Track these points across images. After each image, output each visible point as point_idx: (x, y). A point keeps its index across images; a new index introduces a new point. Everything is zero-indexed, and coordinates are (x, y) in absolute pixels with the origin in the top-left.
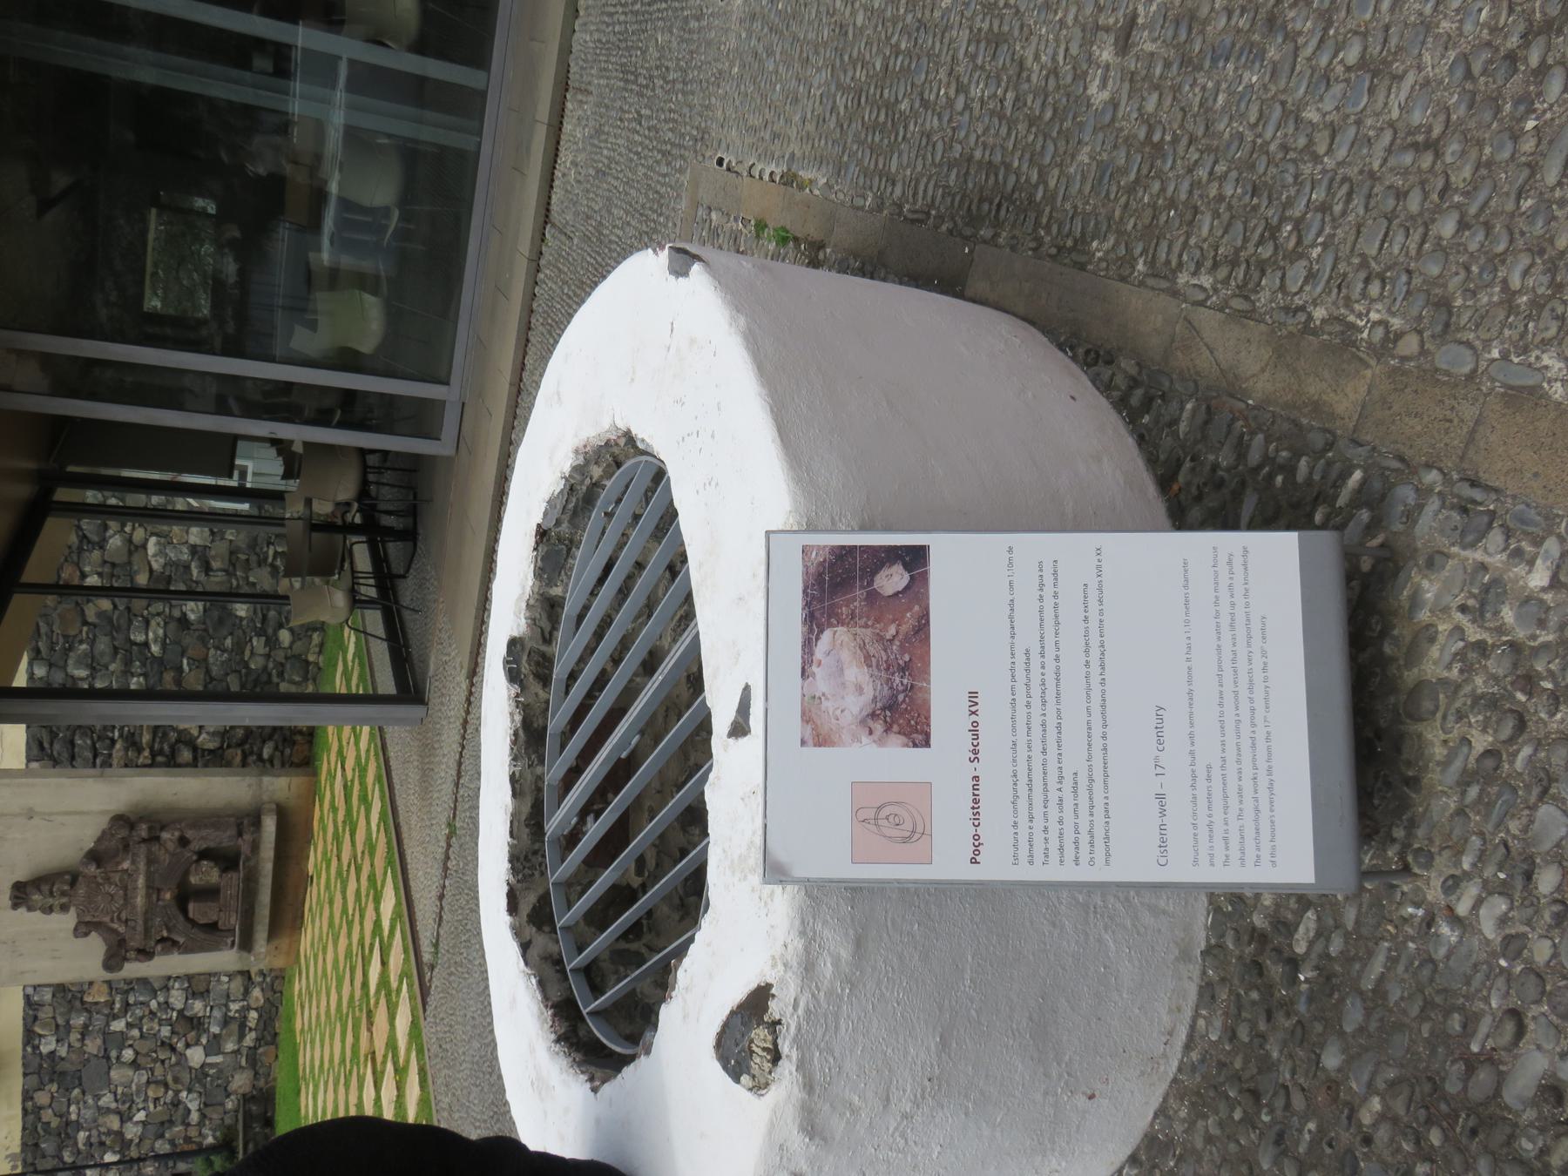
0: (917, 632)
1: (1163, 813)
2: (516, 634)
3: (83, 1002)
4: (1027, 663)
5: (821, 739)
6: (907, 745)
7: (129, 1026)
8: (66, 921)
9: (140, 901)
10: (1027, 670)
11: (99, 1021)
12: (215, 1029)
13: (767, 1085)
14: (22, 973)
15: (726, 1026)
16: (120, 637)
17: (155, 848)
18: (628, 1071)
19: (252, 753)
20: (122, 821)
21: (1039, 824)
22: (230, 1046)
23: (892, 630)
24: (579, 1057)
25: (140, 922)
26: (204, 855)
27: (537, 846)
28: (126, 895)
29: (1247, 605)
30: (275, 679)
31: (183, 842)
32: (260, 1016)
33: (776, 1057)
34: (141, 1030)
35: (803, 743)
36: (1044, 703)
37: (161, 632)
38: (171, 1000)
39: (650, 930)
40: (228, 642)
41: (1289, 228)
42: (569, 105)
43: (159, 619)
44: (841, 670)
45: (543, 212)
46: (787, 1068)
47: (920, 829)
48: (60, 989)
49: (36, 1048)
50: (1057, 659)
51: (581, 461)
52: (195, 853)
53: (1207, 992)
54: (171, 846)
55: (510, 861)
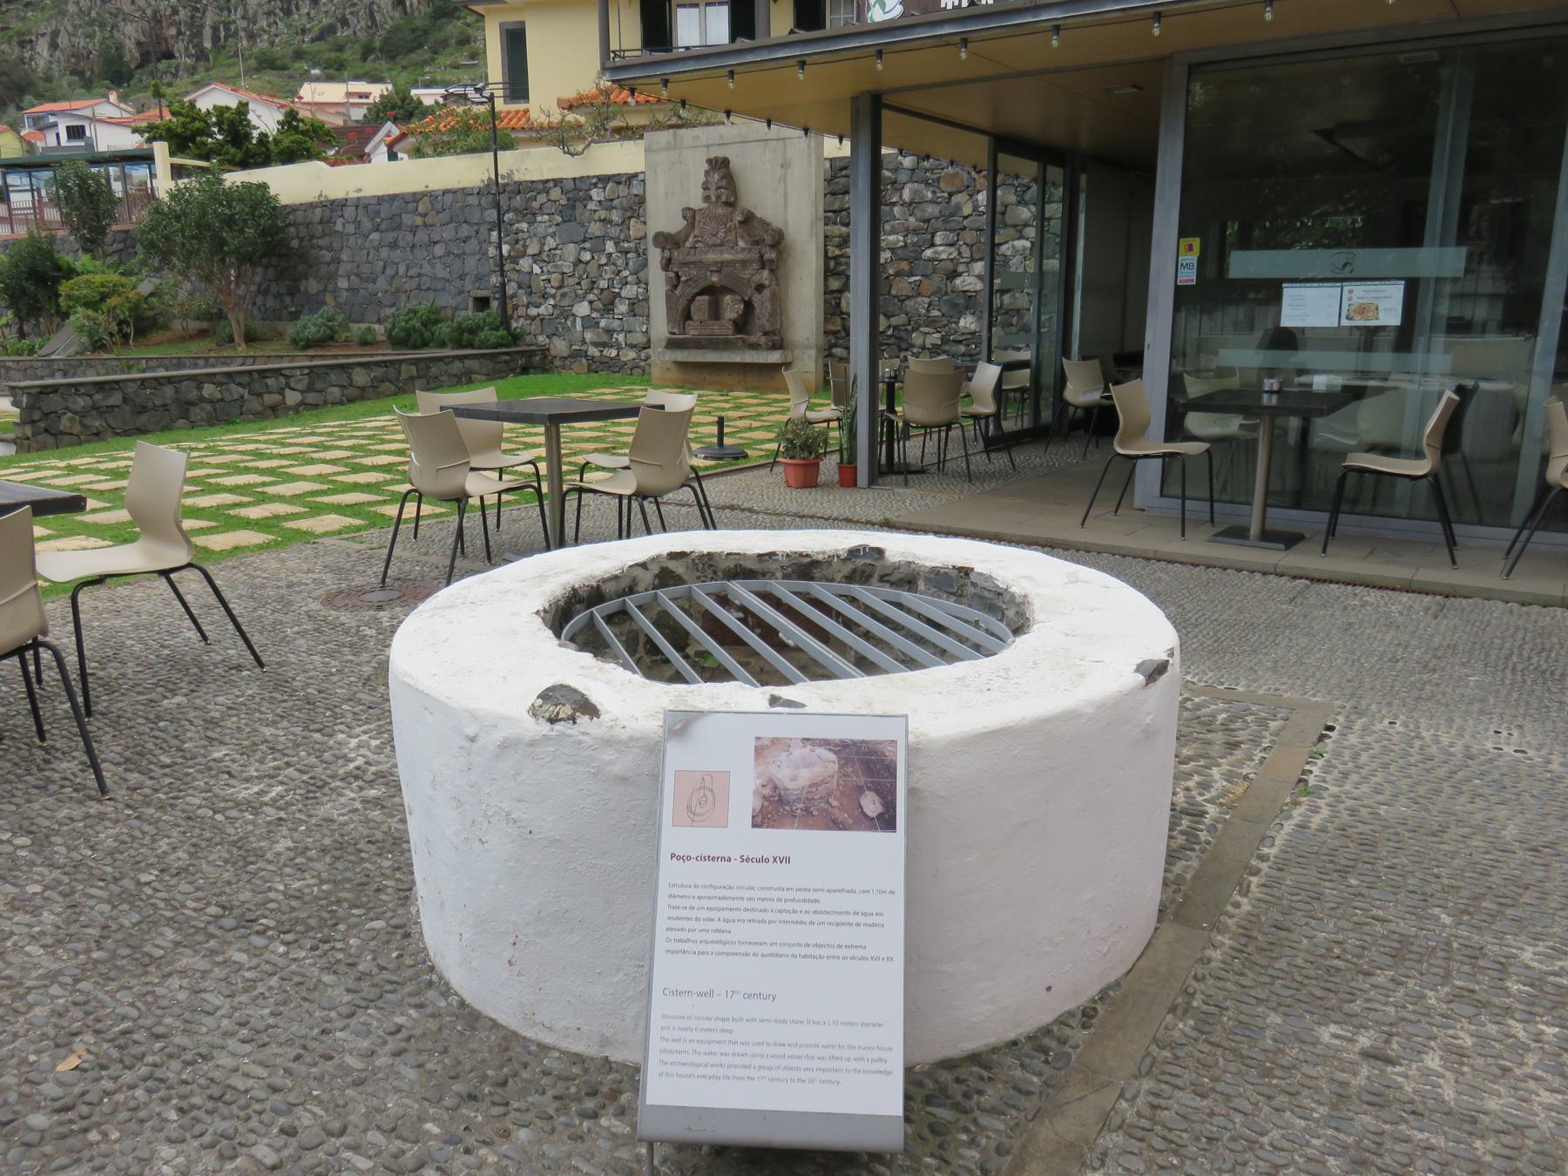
0: (833, 821)
1: (700, 994)
2: (887, 554)
3: (630, 218)
4: (810, 901)
5: (759, 751)
6: (754, 811)
7: (610, 255)
8: (696, 202)
9: (711, 257)
10: (804, 900)
11: (614, 231)
12: (603, 323)
13: (534, 715)
15: (575, 691)
16: (939, 223)
17: (755, 266)
18: (549, 633)
19: (837, 338)
20: (778, 240)
21: (697, 903)
22: (589, 336)
23: (835, 803)
24: (562, 603)
25: (694, 259)
26: (749, 305)
27: (720, 574)
29: (848, 1071)
31: (760, 288)
32: (612, 359)
33: (552, 721)
34: (606, 264)
35: (758, 738)
36: (780, 911)
37: (944, 256)
38: (629, 287)
39: (653, 661)
40: (935, 313)
41: (1175, 1162)
42: (1428, 599)
43: (955, 254)
44: (805, 766)
45: (1324, 577)
46: (545, 727)
47: (696, 818)
48: (641, 200)
49: (595, 185)
50: (812, 923)
51: (1018, 600)
53: (578, 1059)
54: (756, 278)
55: (709, 554)
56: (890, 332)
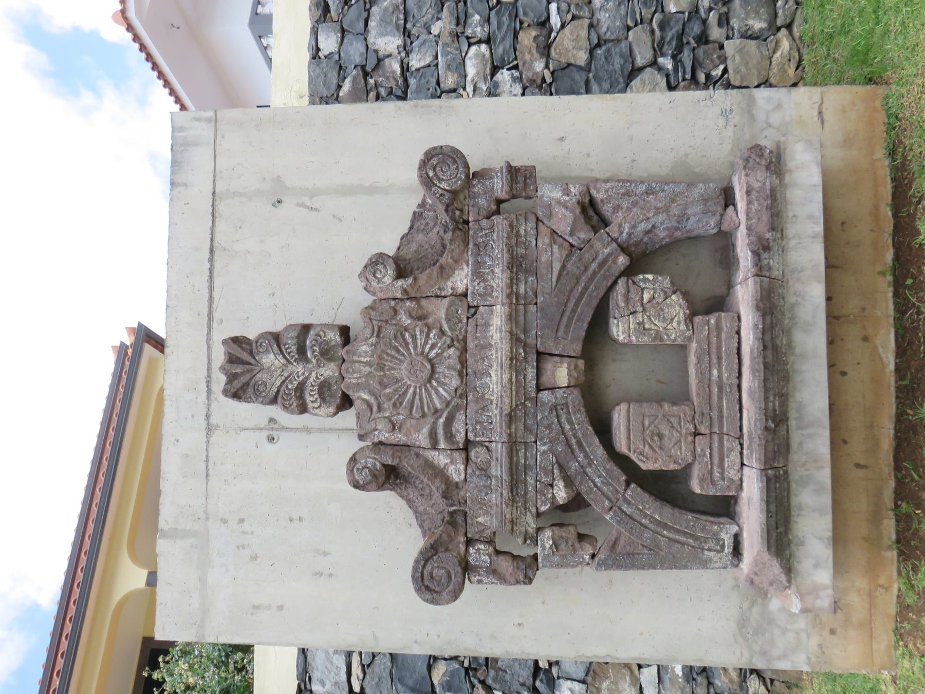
14: (256, 607)
25: (499, 449)
28: (463, 362)
30: (716, 33)
52: (624, 249)
56: (667, 62)
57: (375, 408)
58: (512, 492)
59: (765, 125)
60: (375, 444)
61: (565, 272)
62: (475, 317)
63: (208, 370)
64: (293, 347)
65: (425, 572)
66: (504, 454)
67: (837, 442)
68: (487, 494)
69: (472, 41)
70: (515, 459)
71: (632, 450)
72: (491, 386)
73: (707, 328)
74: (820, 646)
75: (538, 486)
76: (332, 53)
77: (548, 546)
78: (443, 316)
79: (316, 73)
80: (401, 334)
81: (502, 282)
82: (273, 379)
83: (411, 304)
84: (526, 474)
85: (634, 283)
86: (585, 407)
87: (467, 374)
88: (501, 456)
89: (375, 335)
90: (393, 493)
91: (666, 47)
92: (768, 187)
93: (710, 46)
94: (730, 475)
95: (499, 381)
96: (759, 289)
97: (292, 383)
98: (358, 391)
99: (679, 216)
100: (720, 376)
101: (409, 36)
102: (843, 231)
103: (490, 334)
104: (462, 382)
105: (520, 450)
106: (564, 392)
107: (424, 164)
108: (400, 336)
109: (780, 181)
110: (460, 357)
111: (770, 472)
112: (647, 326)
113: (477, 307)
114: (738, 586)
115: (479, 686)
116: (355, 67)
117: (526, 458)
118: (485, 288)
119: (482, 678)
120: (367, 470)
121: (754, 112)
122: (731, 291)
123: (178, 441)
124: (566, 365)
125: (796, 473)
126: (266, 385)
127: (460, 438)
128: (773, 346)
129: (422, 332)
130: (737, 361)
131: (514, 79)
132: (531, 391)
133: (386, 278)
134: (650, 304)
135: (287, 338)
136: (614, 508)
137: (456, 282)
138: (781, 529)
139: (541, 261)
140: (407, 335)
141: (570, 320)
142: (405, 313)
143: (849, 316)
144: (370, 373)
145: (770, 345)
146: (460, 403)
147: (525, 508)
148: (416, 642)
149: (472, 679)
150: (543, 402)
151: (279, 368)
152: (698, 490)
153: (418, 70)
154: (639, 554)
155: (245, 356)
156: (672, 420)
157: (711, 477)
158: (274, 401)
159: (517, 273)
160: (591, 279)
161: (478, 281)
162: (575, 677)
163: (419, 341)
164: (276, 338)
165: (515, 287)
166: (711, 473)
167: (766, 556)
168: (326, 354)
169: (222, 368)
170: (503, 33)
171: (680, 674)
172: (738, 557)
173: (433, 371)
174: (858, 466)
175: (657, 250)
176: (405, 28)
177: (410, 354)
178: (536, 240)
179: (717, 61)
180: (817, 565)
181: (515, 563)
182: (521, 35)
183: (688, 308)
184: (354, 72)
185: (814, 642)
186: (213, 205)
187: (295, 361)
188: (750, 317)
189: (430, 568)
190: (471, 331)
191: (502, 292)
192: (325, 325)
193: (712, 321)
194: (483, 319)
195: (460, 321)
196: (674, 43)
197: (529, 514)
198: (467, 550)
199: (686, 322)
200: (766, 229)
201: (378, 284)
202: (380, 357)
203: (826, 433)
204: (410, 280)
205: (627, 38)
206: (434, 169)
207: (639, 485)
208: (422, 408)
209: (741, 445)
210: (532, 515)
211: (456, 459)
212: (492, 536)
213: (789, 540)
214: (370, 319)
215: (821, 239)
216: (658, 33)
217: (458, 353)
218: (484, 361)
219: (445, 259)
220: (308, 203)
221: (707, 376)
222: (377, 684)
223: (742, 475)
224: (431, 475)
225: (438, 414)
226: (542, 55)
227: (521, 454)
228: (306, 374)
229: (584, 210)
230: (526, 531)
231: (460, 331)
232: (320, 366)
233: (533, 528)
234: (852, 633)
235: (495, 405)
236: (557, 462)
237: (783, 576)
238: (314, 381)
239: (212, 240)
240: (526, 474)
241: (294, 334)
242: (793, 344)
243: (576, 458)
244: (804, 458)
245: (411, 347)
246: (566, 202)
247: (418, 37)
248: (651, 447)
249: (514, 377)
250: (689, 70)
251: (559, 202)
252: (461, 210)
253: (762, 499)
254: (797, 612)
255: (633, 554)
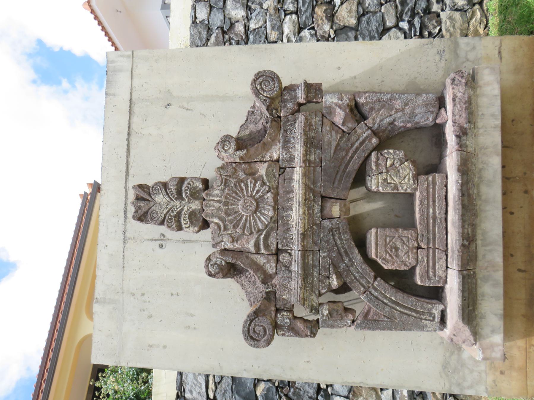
14: (151, 346)
25: (297, 254)
28: (276, 201)
52: (375, 133)
56: (404, 25)
57: (222, 228)
58: (304, 281)
59: (465, 60)
60: (222, 250)
61: (339, 148)
62: (283, 174)
63: (125, 204)
64: (174, 191)
65: (251, 328)
66: (300, 257)
67: (507, 256)
68: (289, 282)
69: (287, 12)
70: (306, 261)
71: (378, 257)
72: (293, 216)
73: (426, 183)
74: (494, 381)
75: (320, 278)
76: (204, 20)
77: (325, 314)
78: (265, 174)
79: (194, 32)
80: (239, 184)
81: (300, 153)
82: (162, 210)
83: (245, 166)
84: (313, 270)
85: (382, 155)
86: (350, 230)
87: (278, 209)
88: (298, 259)
89: (223, 184)
90: (233, 280)
91: (404, 16)
92: (466, 96)
93: (432, 15)
94: (439, 274)
95: (297, 213)
96: (459, 159)
97: (173, 213)
98: (212, 217)
99: (410, 114)
100: (434, 212)
101: (250, 10)
102: (513, 125)
103: (293, 185)
104: (275, 213)
105: (309, 255)
106: (337, 221)
107: (254, 81)
108: (238, 185)
109: (474, 93)
110: (273, 198)
111: (465, 272)
112: (389, 181)
113: (285, 168)
114: (443, 343)
115: (284, 397)
116: (218, 28)
117: (313, 261)
118: (290, 157)
119: (286, 393)
120: (216, 265)
121: (458, 52)
122: (442, 161)
123: (107, 246)
124: (338, 204)
125: (481, 274)
126: (158, 214)
127: (273, 247)
128: (468, 194)
129: (251, 182)
130: (445, 203)
131: (312, 35)
132: (317, 220)
133: (230, 150)
134: (391, 168)
135: (171, 185)
136: (367, 293)
137: (273, 152)
138: (471, 308)
139: (324, 141)
140: (242, 184)
141: (342, 177)
142: (242, 171)
143: (516, 177)
144: (220, 207)
145: (466, 194)
146: (274, 226)
147: (312, 291)
148: (245, 370)
149: (280, 393)
150: (324, 227)
151: (166, 203)
152: (419, 283)
153: (254, 30)
154: (381, 321)
155: (146, 196)
156: (404, 239)
157: (428, 275)
158: (162, 223)
159: (309, 148)
160: (355, 152)
161: (285, 152)
162: (342, 394)
163: (249, 188)
164: (165, 185)
165: (308, 156)
166: (427, 272)
167: (461, 324)
168: (195, 195)
169: (133, 203)
170: (306, 7)
171: (406, 395)
172: (443, 324)
173: (258, 206)
174: (520, 270)
175: (396, 135)
176: (247, 5)
177: (244, 196)
178: (322, 128)
179: (436, 24)
180: (493, 331)
181: (305, 325)
182: (316, 9)
183: (415, 170)
184: (217, 31)
185: (490, 379)
186: (130, 107)
187: (175, 199)
188: (454, 176)
189: (253, 326)
190: (281, 183)
191: (300, 159)
192: (193, 178)
193: (430, 179)
194: (288, 175)
195: (275, 177)
196: (409, 13)
197: (314, 294)
198: (276, 315)
199: (413, 179)
200: (464, 122)
201: (225, 153)
202: (226, 198)
203: (501, 249)
204: (245, 151)
205: (380, 11)
206: (261, 84)
207: (382, 279)
208: (251, 228)
209: (447, 255)
210: (316, 295)
211: (270, 260)
212: (291, 307)
213: (476, 315)
214: (221, 175)
215: (499, 129)
216: (399, 7)
217: (272, 196)
218: (289, 201)
219: (267, 138)
220: (186, 106)
221: (426, 212)
222: (224, 394)
223: (447, 274)
224: (255, 269)
225: (260, 233)
226: (329, 21)
227: (310, 258)
228: (182, 207)
229: (351, 110)
230: (312, 305)
231: (275, 183)
232: (190, 203)
233: (316, 303)
234: (514, 374)
235: (294, 228)
236: (332, 263)
237: (472, 337)
238: (186, 211)
239: (129, 127)
240: (313, 270)
241: (175, 183)
242: (480, 194)
243: (344, 261)
244: (486, 264)
245: (245, 191)
246: (340, 105)
247: (255, 10)
248: (390, 255)
249: (307, 211)
250: (418, 29)
251: (336, 105)
252: (277, 110)
253: (459, 289)
254: (480, 360)
255: (378, 321)
